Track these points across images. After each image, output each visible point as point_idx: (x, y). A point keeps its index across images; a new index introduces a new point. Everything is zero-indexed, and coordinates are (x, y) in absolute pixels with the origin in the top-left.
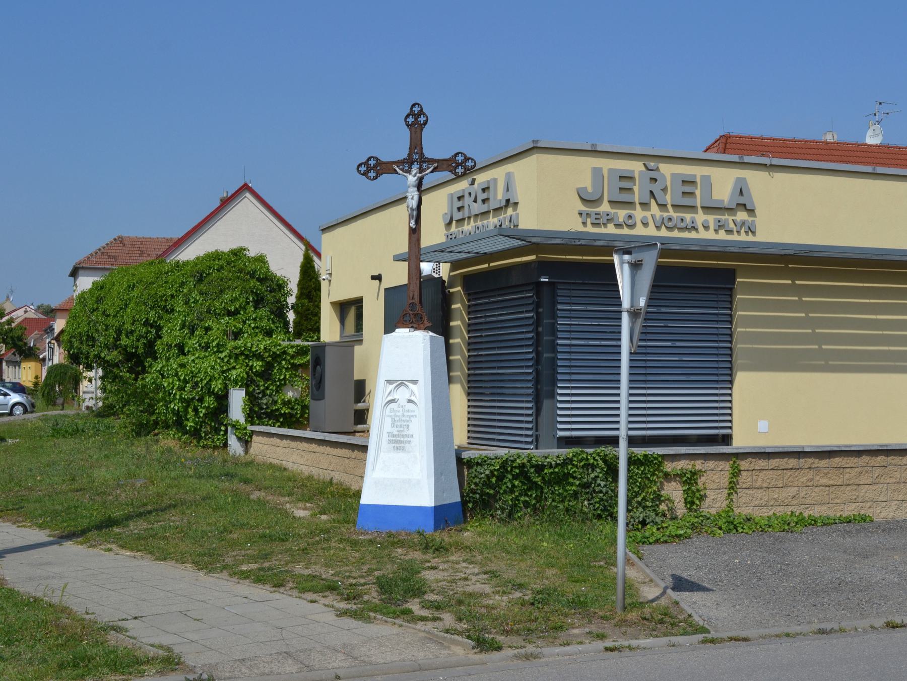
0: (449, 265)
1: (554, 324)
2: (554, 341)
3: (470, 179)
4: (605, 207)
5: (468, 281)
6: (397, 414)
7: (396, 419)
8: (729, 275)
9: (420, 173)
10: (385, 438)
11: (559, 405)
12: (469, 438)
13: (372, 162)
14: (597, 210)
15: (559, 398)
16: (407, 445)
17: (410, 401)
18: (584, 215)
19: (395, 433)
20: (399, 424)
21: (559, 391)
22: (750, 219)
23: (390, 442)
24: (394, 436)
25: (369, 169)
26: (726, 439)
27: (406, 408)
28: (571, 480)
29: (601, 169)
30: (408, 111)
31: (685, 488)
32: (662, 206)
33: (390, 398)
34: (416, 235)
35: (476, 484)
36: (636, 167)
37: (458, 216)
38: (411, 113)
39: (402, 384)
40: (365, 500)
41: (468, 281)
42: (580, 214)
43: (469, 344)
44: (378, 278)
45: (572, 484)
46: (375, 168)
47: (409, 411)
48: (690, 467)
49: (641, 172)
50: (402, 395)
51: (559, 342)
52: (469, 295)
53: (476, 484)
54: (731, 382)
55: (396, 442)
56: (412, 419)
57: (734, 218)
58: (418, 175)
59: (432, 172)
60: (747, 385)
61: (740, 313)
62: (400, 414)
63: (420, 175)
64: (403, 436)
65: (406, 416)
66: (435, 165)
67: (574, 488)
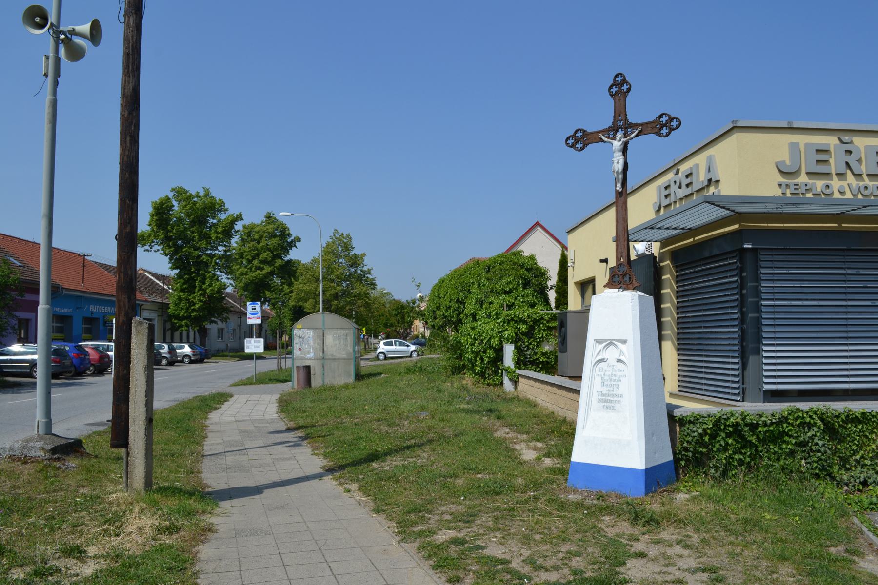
0: (659, 244)
1: (757, 287)
2: (758, 302)
3: (675, 171)
4: (803, 179)
5: (675, 256)
7: (606, 378)
10: (595, 397)
11: (765, 361)
13: (579, 134)
14: (796, 181)
15: (765, 354)
16: (617, 405)
17: (619, 361)
18: (784, 186)
20: (608, 383)
21: (765, 348)
23: (600, 401)
24: (603, 395)
28: (786, 438)
30: (611, 82)
32: (858, 176)
33: (599, 357)
34: (623, 198)
35: (688, 442)
36: (831, 141)
37: (665, 202)
38: (615, 84)
39: (611, 343)
41: (675, 256)
42: (780, 185)
43: (678, 308)
44: (605, 261)
45: (787, 443)
46: (581, 140)
47: (618, 370)
49: (835, 146)
50: (611, 354)
51: (764, 303)
52: (677, 267)
53: (688, 442)
55: (606, 401)
59: (637, 136)
62: (610, 373)
64: (613, 395)
65: (616, 376)
66: (640, 128)
67: (790, 446)
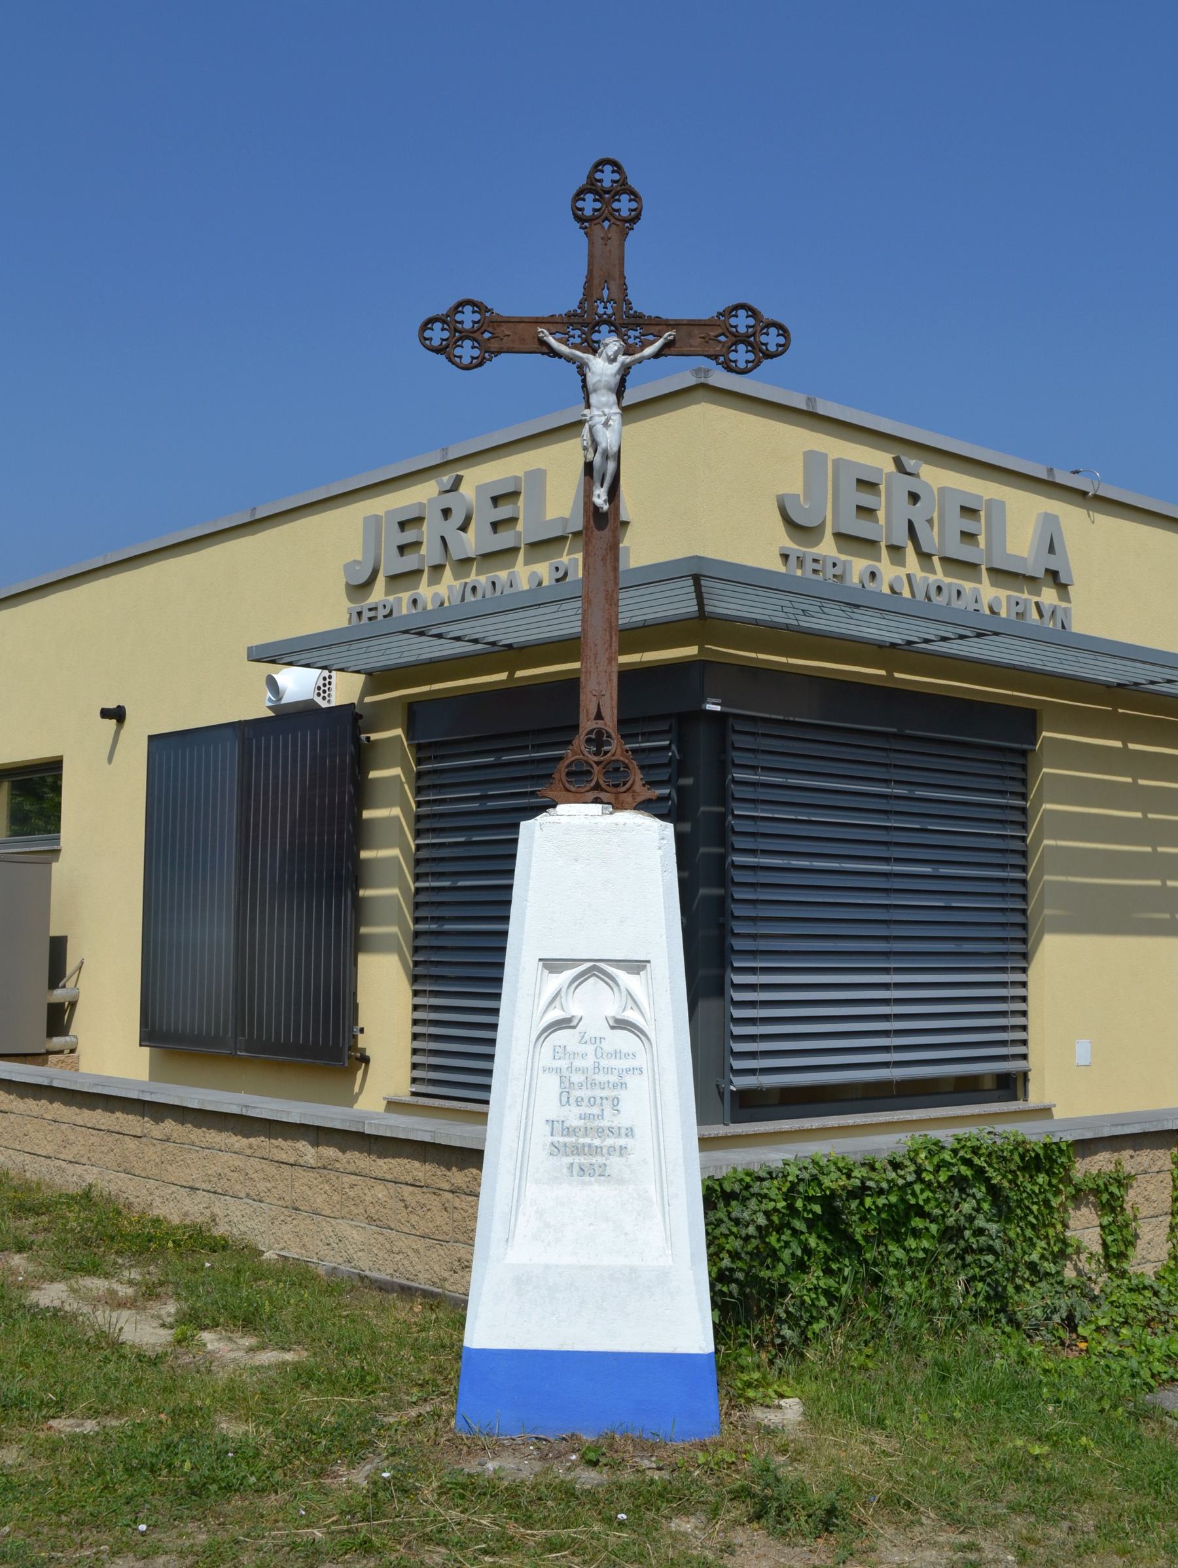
1: (723, 817)
2: (723, 858)
3: (447, 479)
4: (827, 547)
5: (414, 714)
6: (578, 1063)
7: (577, 1078)
8: (1026, 722)
9: (626, 353)
10: (541, 1136)
11: (738, 1013)
12: (414, 1080)
13: (468, 318)
14: (814, 550)
15: (738, 996)
16: (615, 1162)
17: (621, 1024)
18: (793, 560)
19: (574, 1122)
20: (585, 1093)
21: (738, 979)
22: (1064, 605)
23: (556, 1149)
24: (569, 1131)
25: (460, 335)
26: (1010, 1085)
27: (607, 1047)
28: (918, 1223)
29: (826, 455)
30: (582, 181)
31: (1106, 1220)
32: (924, 557)
33: (555, 1014)
34: (607, 533)
35: (735, 1256)
36: (879, 461)
37: (394, 564)
38: (591, 187)
39: (595, 969)
40: (484, 1331)
41: (414, 714)
42: (785, 557)
43: (418, 862)
45: (916, 1233)
46: (473, 334)
47: (617, 1054)
48: (1112, 1167)
49: (889, 475)
50: (593, 1004)
51: (739, 859)
52: (419, 748)
53: (735, 1256)
54: (1025, 956)
55: (578, 1150)
56: (628, 1078)
57: (1036, 599)
58: (621, 358)
59: (657, 355)
60: (1062, 967)
61: (1047, 806)
62: (589, 1062)
63: (628, 359)
64: (600, 1132)
65: (609, 1070)
66: (669, 335)
67: (925, 1244)
